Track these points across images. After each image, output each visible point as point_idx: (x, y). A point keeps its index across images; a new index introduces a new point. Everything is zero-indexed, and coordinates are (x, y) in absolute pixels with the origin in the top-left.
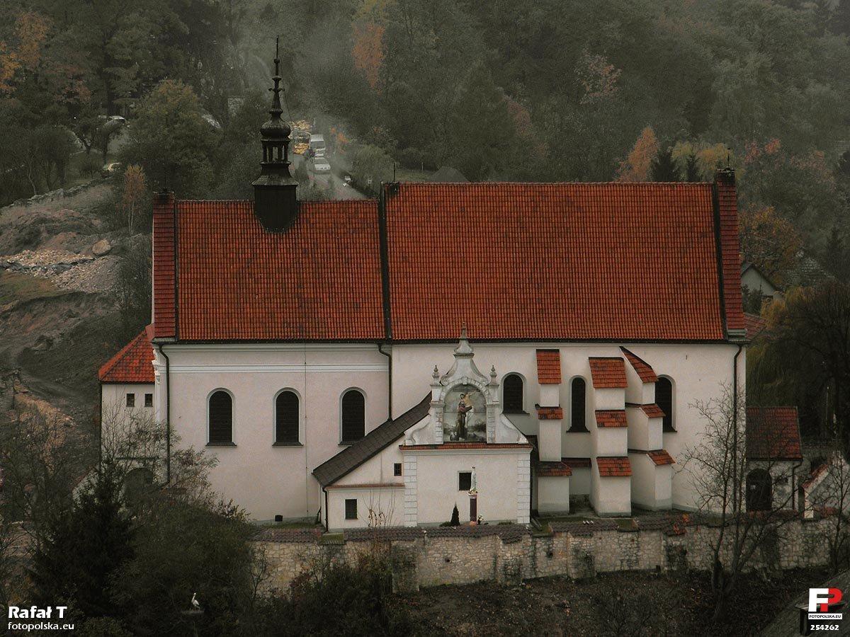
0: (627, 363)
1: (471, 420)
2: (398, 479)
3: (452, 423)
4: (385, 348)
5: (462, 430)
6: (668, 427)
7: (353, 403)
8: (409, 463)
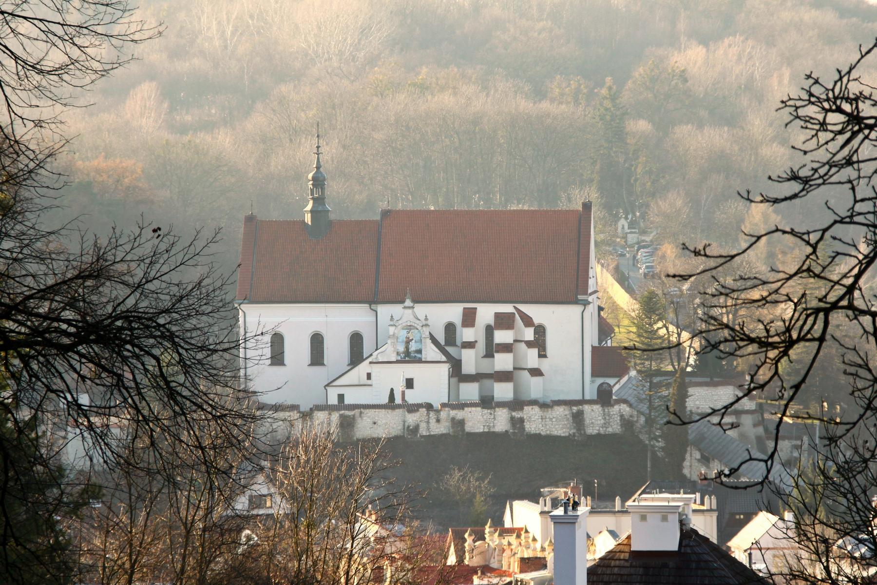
0: (517, 316)
1: (413, 347)
2: (369, 382)
3: (401, 348)
4: (373, 307)
5: (407, 353)
6: (542, 355)
7: (356, 340)
8: (375, 370)
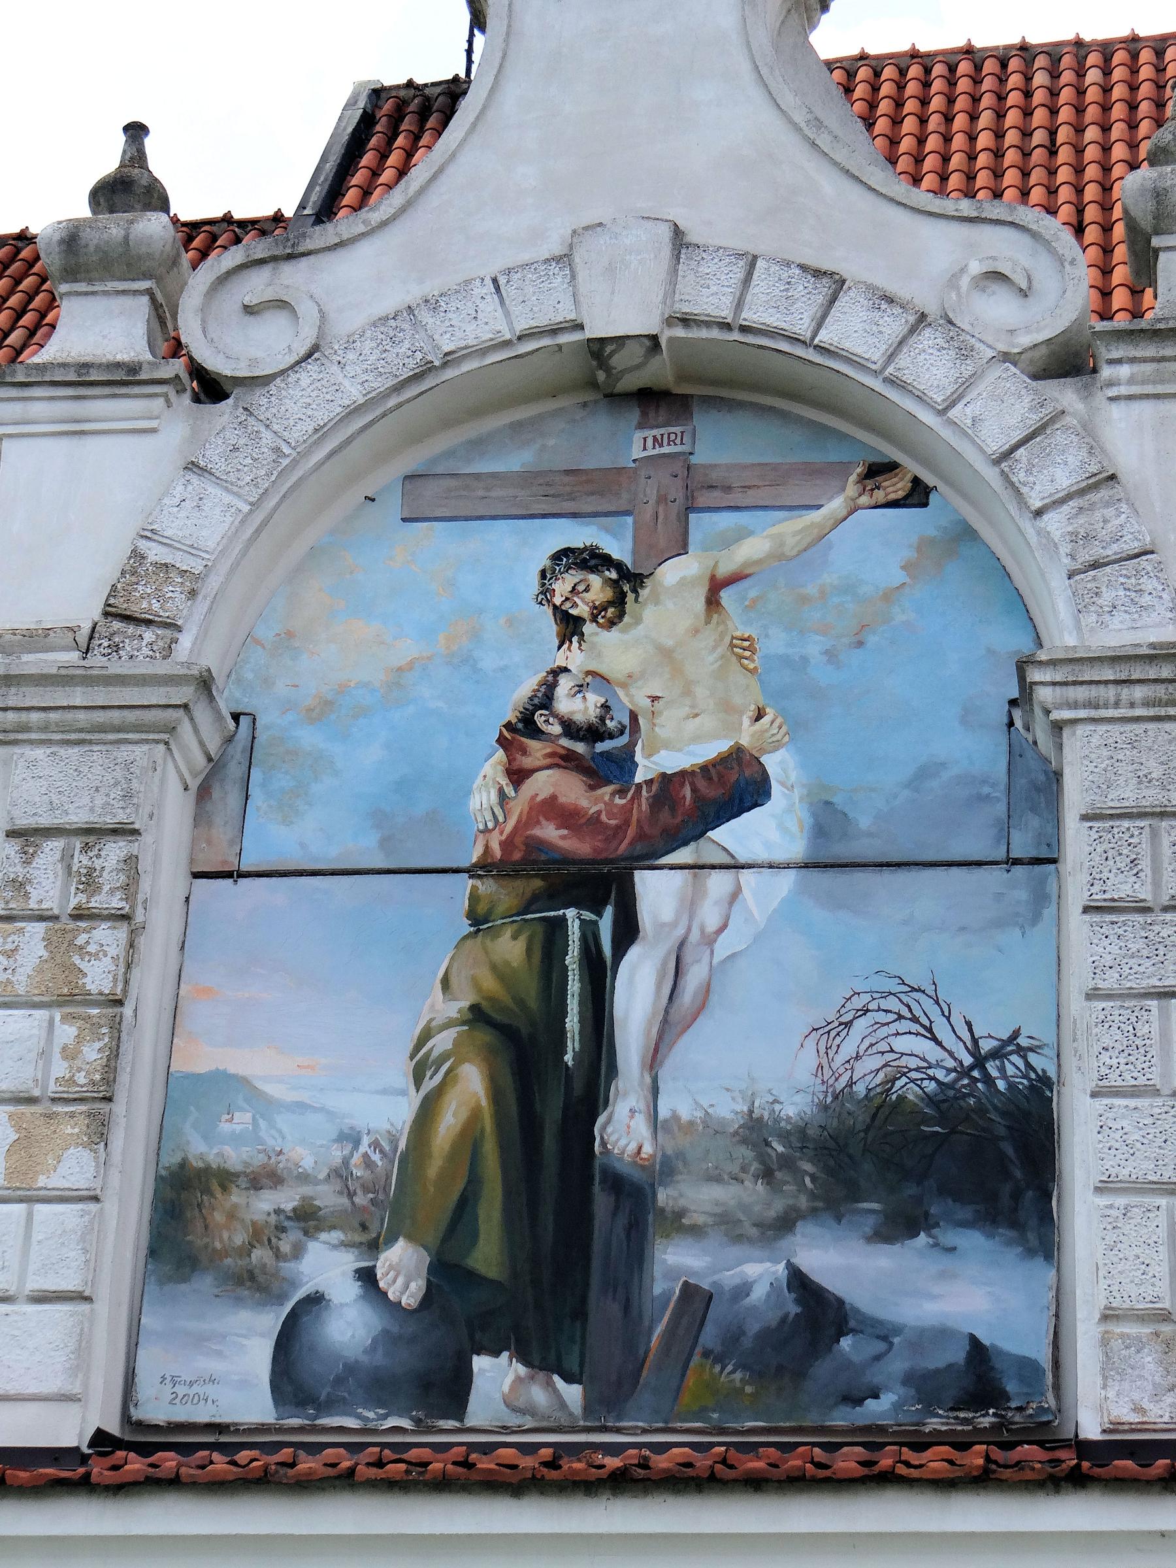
1: (742, 1011)
3: (336, 1053)
